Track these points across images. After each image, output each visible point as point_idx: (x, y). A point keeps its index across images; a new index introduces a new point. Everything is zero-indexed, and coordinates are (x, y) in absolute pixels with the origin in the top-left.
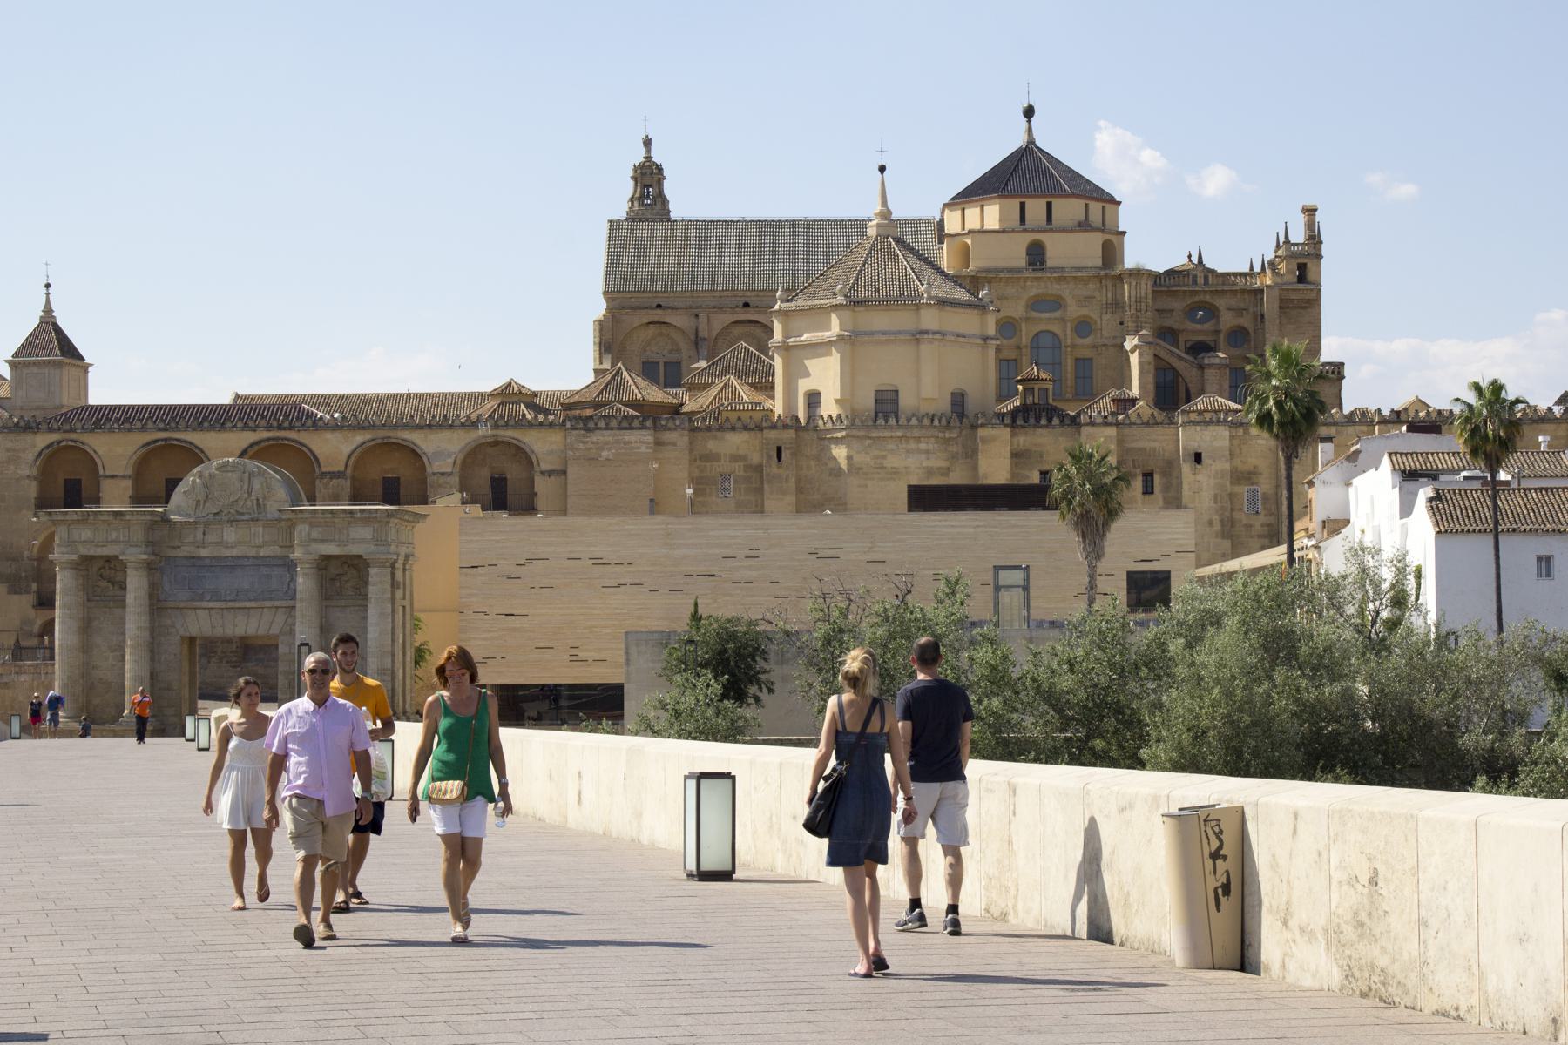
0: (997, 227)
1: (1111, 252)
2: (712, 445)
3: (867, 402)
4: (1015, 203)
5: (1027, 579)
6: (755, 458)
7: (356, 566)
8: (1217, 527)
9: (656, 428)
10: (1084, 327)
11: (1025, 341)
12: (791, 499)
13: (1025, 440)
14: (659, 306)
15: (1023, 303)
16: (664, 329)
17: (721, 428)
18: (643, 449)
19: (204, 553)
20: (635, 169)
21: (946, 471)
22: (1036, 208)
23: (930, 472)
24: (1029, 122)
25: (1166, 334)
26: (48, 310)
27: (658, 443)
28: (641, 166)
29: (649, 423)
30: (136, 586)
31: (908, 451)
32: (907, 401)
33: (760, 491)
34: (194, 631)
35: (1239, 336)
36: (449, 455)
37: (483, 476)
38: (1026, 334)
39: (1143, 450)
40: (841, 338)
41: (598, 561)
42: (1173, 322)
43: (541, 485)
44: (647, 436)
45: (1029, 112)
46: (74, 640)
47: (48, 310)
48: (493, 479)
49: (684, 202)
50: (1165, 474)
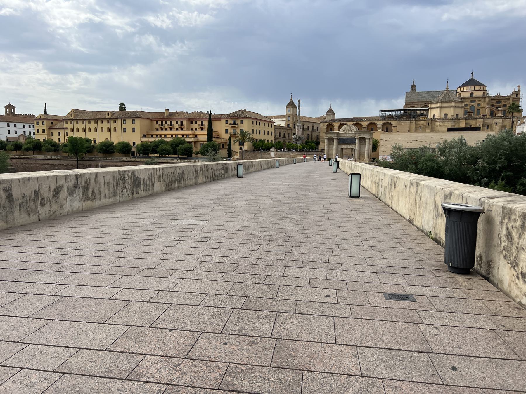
2: (419, 122)
3: (442, 116)
6: (425, 124)
10: (479, 105)
13: (467, 121)
21: (455, 126)
22: (472, 88)
23: (452, 126)
26: (331, 107)
27: (410, 122)
30: (335, 141)
32: (449, 116)
34: (342, 148)
35: (505, 106)
37: (385, 127)
38: (469, 106)
39: (487, 122)
40: (439, 107)
41: (400, 138)
42: (494, 104)
44: (408, 122)
46: (327, 149)
47: (331, 107)
49: (418, 89)
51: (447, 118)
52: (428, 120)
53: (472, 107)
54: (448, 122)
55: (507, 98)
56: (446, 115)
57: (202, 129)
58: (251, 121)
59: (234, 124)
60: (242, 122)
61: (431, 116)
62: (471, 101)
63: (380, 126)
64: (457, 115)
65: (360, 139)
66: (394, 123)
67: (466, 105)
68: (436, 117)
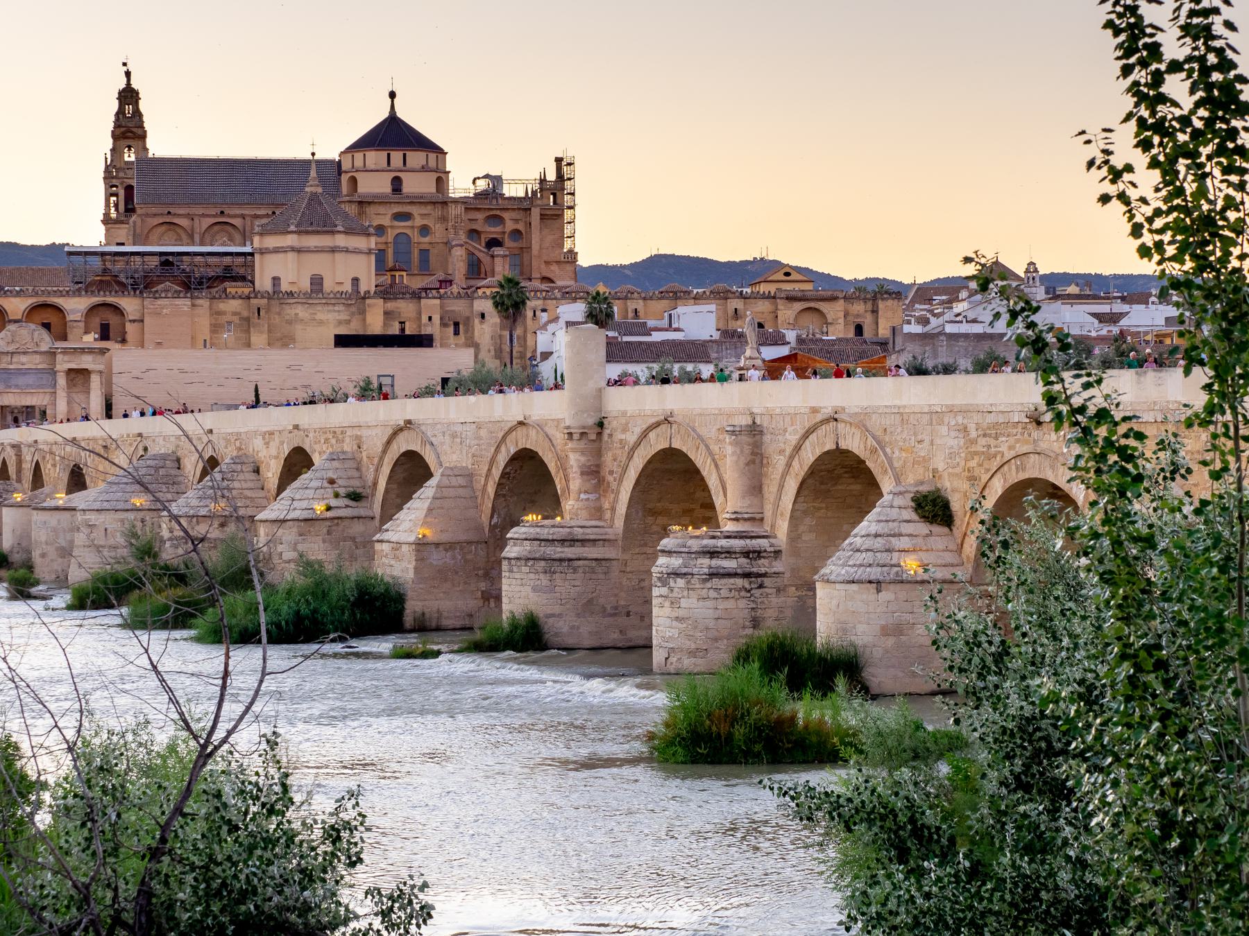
0: (373, 167)
1: (442, 180)
3: (305, 285)
4: (385, 154)
5: (393, 381)
6: (245, 314)
7: (84, 373)
8: (493, 353)
9: (192, 298)
10: (425, 230)
11: (390, 239)
12: (265, 336)
13: (391, 305)
14: (169, 213)
15: (389, 216)
16: (172, 227)
17: (227, 297)
18: (186, 309)
19: (11, 367)
20: (120, 93)
22: (397, 156)
24: (392, 102)
25: (474, 233)
27: (193, 305)
28: (124, 89)
29: (189, 295)
31: (329, 311)
32: (328, 285)
33: (248, 331)
35: (516, 234)
36: (78, 311)
37: (96, 322)
38: (390, 235)
41: (182, 371)
43: (130, 328)
44: (188, 302)
45: (392, 95)
48: (102, 324)
50: (465, 325)
51: (321, 291)
52: (256, 297)
54: (326, 308)
56: (317, 282)
61: (263, 282)
62: (399, 217)
63: (78, 316)
64: (356, 281)
65: (70, 371)
66: (129, 304)
67: (380, 230)
68: (285, 287)
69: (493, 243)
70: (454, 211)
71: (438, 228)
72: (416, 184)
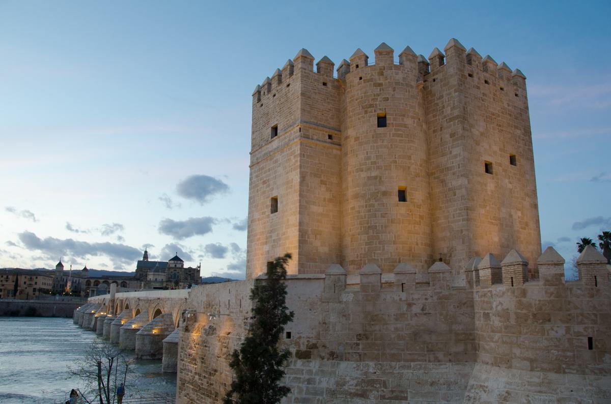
1: (183, 265)
3: (154, 280)
10: (178, 272)
22: (176, 262)
35: (193, 274)
38: (173, 273)
44: (136, 282)
53: (175, 274)
55: (194, 269)
56: (156, 279)
57: (7, 281)
58: (42, 277)
59: (31, 278)
60: (37, 278)
61: (148, 279)
62: (174, 270)
67: (172, 272)
69: (189, 275)
70: (183, 270)
71: (180, 272)
72: (178, 266)
